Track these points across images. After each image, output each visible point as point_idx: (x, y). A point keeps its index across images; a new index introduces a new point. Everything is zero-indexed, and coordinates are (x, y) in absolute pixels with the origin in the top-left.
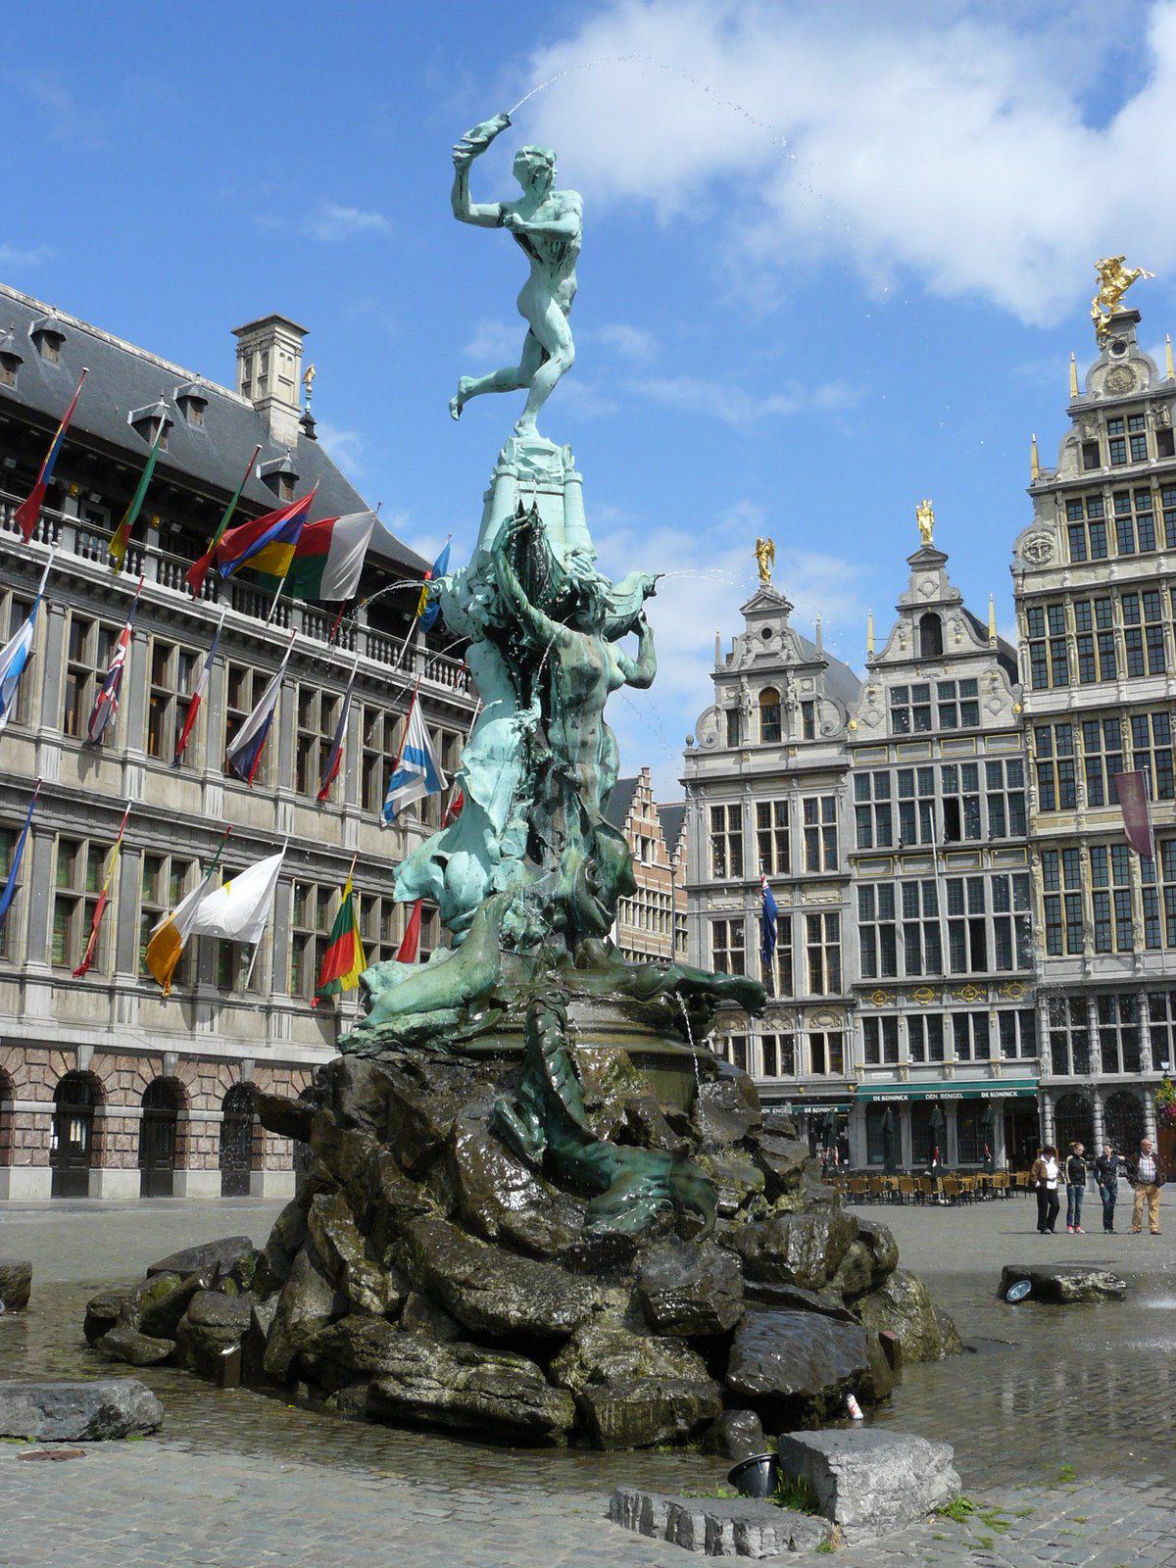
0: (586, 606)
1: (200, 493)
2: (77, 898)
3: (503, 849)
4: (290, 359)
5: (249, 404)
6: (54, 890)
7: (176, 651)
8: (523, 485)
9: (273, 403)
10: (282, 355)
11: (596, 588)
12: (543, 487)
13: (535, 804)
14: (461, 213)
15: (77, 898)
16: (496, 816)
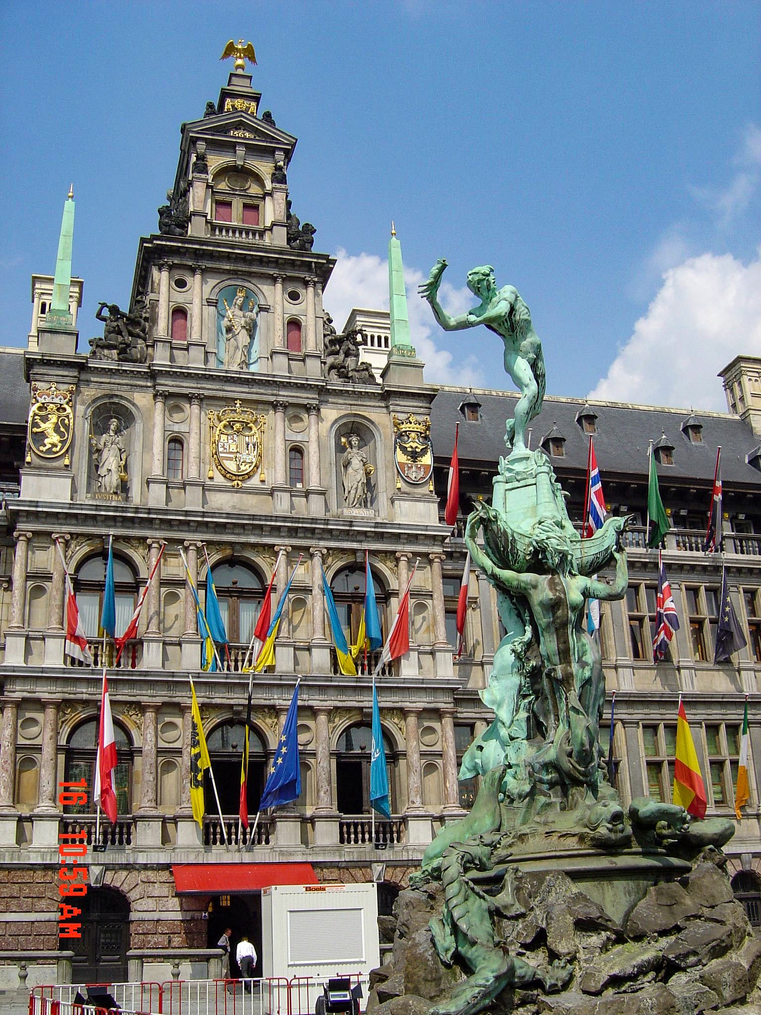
0: (545, 557)
1: (692, 487)
2: (663, 762)
3: (512, 735)
4: (756, 380)
5: (737, 417)
6: (644, 759)
7: (702, 589)
8: (509, 486)
9: (751, 412)
10: (750, 380)
11: (547, 544)
12: (522, 483)
13: (537, 698)
14: (447, 327)
15: (663, 762)
16: (504, 714)
